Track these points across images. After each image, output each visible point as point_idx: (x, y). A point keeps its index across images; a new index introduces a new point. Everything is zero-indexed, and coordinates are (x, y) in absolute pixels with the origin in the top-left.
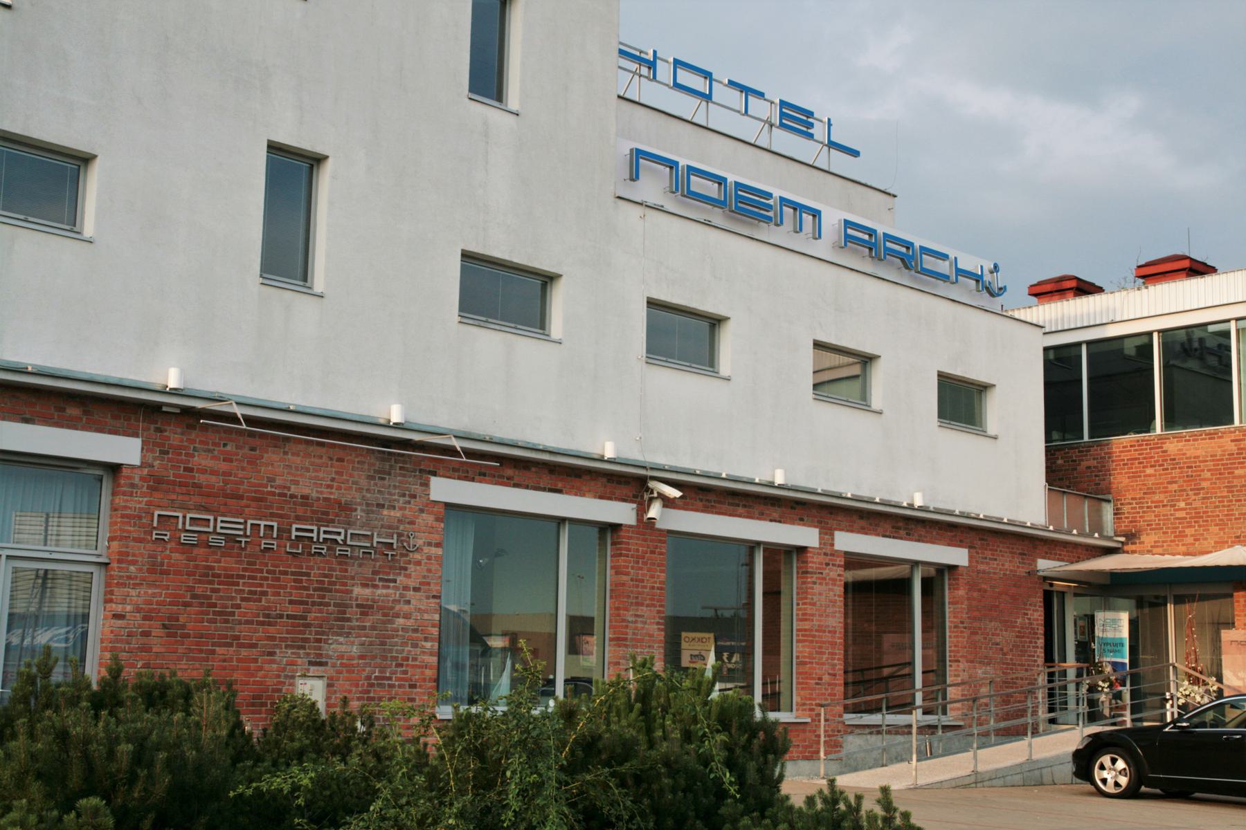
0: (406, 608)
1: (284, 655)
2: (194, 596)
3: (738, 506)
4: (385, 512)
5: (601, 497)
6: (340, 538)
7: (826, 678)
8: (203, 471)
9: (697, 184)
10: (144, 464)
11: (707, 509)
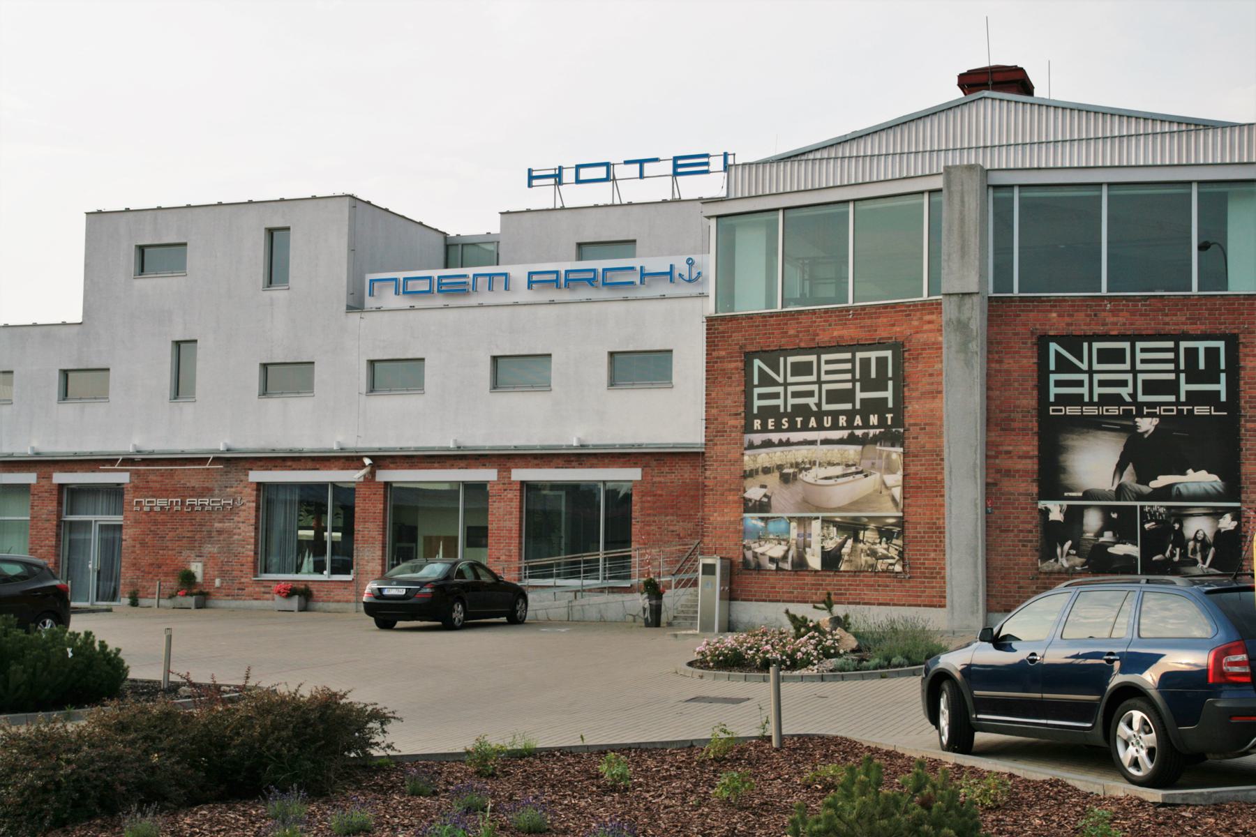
0: (238, 531)
1: (185, 553)
2: (151, 531)
3: (434, 463)
4: (228, 489)
5: (342, 469)
6: (207, 503)
7: (503, 558)
8: (154, 482)
9: (411, 286)
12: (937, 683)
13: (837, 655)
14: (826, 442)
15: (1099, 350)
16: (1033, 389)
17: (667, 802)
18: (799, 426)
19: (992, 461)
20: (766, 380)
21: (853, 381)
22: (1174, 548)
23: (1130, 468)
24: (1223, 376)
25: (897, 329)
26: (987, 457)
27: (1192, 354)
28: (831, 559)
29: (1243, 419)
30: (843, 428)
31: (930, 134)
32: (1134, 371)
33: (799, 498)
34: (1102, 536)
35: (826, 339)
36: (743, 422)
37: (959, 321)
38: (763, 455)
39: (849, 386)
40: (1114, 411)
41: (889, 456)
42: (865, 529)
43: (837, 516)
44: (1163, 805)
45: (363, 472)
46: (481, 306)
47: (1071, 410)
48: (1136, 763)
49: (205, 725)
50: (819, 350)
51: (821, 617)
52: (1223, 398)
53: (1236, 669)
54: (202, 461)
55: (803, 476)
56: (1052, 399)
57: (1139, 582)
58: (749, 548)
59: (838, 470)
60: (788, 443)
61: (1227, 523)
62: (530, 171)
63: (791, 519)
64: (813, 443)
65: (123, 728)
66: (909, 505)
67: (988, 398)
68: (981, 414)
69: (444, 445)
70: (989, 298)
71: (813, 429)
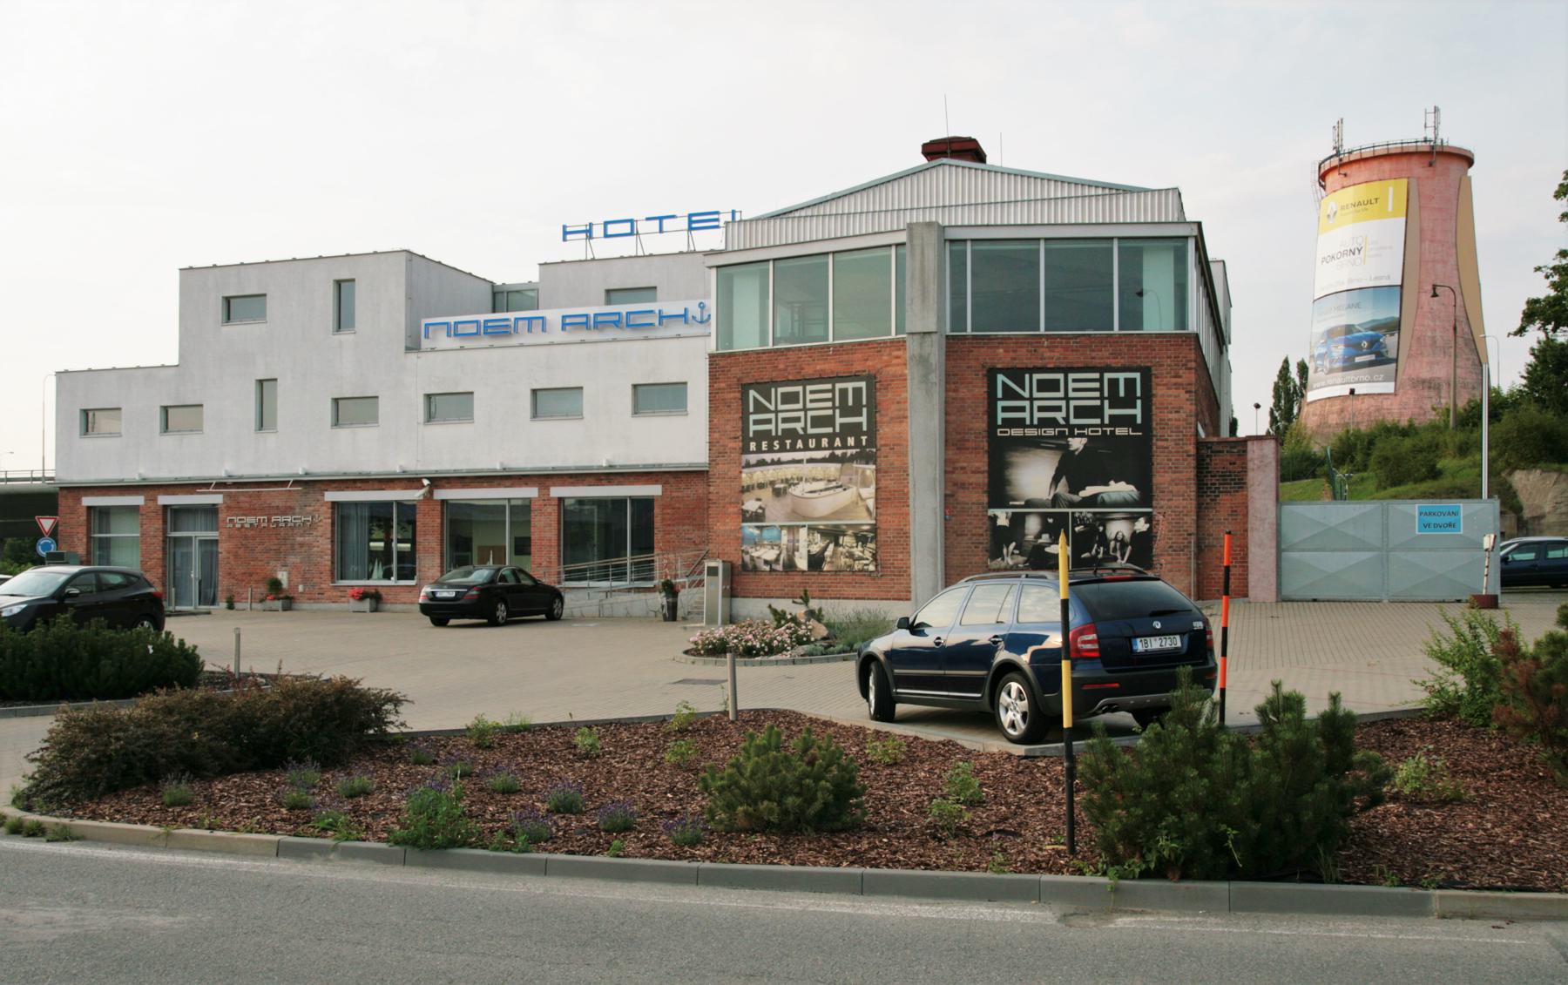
1: (273, 563)
7: (544, 564)
9: (461, 329)
10: (225, 502)
11: (463, 487)
12: (867, 663)
13: (809, 642)
14: (811, 461)
15: (1038, 381)
16: (984, 414)
17: (628, 766)
18: (788, 447)
19: (949, 475)
20: (760, 408)
21: (834, 408)
22: (1099, 547)
23: (1064, 481)
24: (1139, 402)
25: (870, 363)
26: (946, 472)
27: (1114, 383)
28: (816, 561)
29: (1154, 439)
30: (825, 449)
31: (898, 196)
32: (1067, 398)
33: (789, 509)
34: (1040, 537)
35: (811, 372)
36: (741, 444)
37: (921, 356)
38: (759, 473)
39: (830, 412)
40: (1051, 432)
41: (864, 472)
42: (844, 535)
43: (821, 524)
44: (1026, 757)
45: (422, 492)
46: (522, 345)
47: (1016, 432)
48: (1013, 725)
49: (239, 708)
50: (804, 381)
51: (799, 611)
52: (1139, 421)
53: (1089, 646)
54: (284, 483)
55: (791, 490)
56: (999, 422)
57: (1019, 577)
58: (747, 553)
59: (821, 485)
60: (779, 462)
61: (1141, 525)
62: (564, 227)
63: (782, 527)
64: (800, 461)
65: (169, 711)
66: (881, 514)
67: (946, 422)
68: (940, 435)
69: (491, 466)
70: (947, 336)
71: (800, 450)
